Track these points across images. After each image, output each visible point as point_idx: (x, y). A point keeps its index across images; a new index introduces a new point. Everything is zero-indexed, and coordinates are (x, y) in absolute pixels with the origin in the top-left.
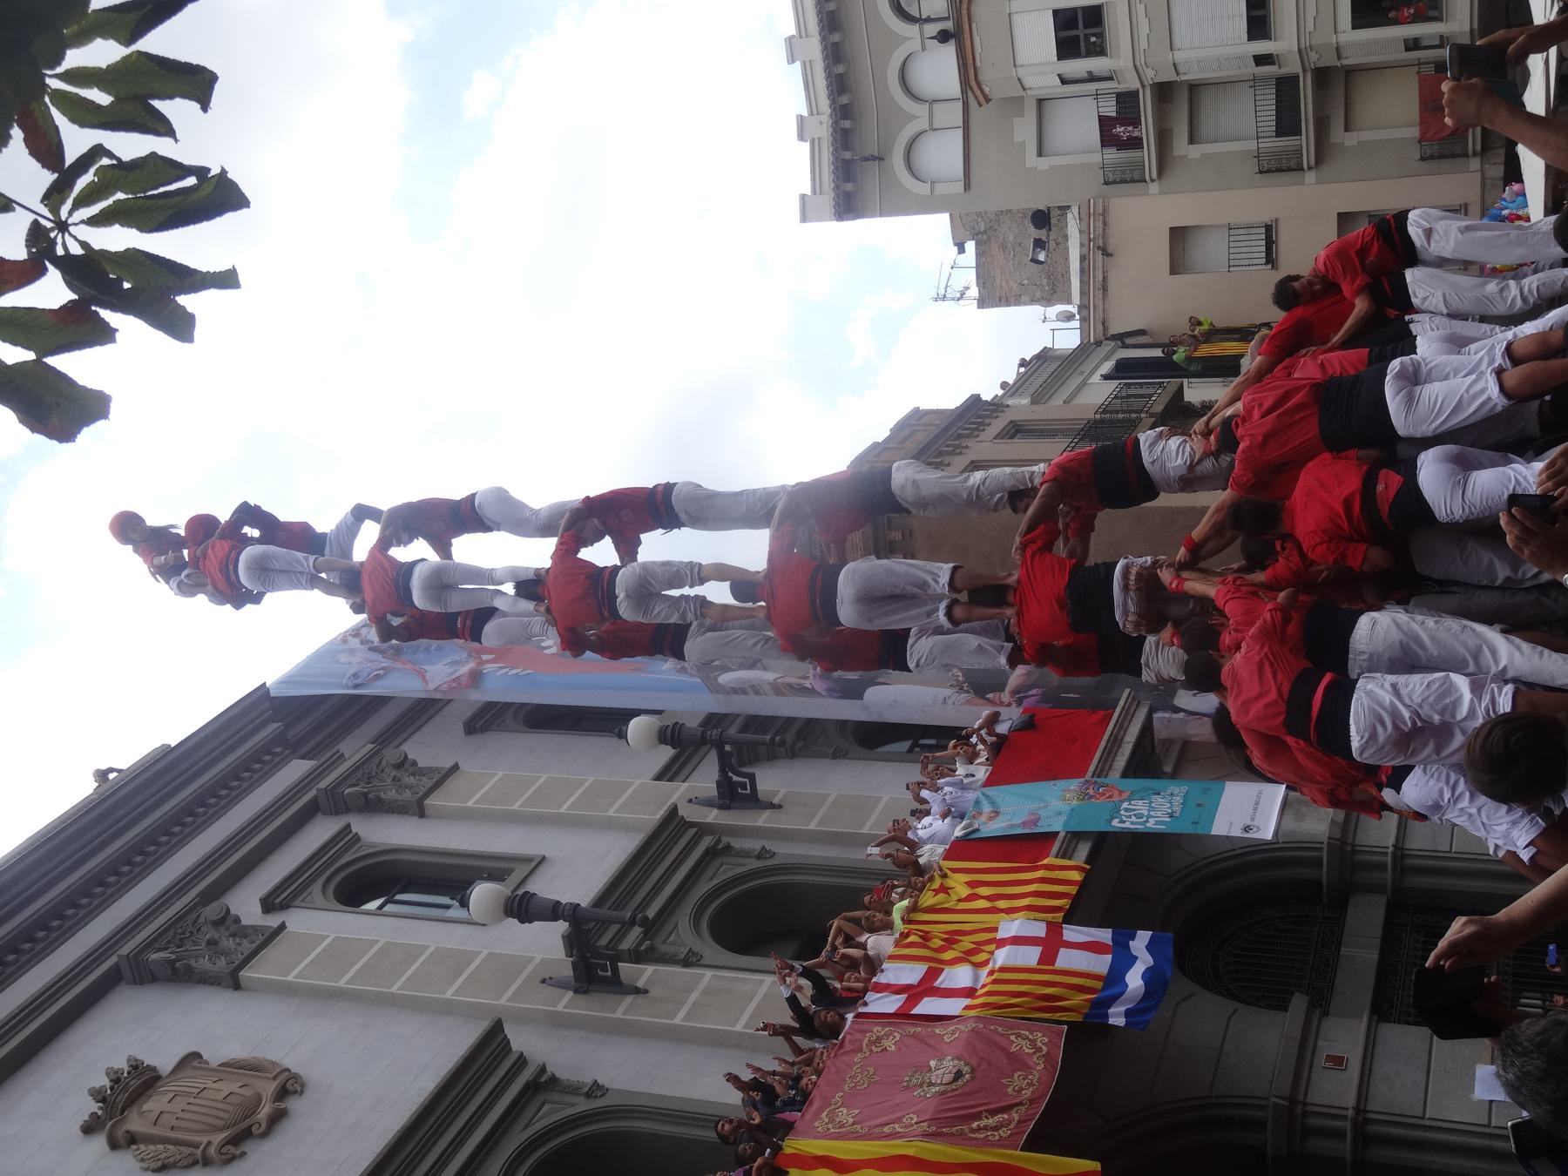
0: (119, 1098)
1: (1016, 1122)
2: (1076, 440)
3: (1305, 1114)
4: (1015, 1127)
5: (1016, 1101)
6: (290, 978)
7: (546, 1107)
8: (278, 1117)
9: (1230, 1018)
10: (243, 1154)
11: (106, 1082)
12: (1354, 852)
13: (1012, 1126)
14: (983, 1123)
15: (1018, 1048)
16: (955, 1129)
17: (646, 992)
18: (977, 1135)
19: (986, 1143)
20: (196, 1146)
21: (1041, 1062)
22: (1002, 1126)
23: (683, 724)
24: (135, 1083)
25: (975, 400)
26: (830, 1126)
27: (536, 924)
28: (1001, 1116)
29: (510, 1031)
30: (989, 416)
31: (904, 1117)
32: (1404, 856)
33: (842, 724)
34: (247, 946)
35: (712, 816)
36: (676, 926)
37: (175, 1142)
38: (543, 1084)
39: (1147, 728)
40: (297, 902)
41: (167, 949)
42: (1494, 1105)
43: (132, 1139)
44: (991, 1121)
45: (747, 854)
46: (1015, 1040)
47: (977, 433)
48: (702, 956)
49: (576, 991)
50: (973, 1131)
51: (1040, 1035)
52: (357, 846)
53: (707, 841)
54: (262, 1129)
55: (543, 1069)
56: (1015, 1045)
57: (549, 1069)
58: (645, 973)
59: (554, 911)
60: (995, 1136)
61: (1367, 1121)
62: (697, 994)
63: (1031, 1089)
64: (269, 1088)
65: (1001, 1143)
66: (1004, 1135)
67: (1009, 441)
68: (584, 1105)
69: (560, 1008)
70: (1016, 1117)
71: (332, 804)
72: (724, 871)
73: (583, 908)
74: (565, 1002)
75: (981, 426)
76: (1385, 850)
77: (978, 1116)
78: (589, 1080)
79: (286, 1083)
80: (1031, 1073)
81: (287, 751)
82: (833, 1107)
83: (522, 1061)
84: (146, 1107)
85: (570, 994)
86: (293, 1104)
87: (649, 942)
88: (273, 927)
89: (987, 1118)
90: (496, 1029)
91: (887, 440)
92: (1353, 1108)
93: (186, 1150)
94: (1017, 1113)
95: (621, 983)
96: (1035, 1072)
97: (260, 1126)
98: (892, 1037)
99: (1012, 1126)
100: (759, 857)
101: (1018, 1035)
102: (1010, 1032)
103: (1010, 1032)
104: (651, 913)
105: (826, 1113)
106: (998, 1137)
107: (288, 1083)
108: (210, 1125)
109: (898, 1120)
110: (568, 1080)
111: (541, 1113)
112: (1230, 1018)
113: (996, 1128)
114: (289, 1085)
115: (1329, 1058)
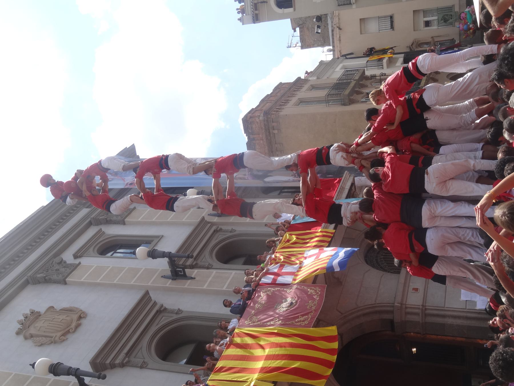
0: (27, 324)
1: (310, 318)
2: (331, 90)
3: (406, 308)
4: (310, 320)
5: (310, 311)
6: (82, 280)
7: (164, 318)
8: (78, 326)
9: (381, 277)
10: (67, 339)
11: (23, 318)
13: (309, 320)
14: (299, 320)
15: (311, 293)
16: (290, 322)
17: (195, 278)
18: (298, 324)
19: (300, 326)
20: (52, 337)
21: (318, 297)
22: (306, 320)
23: (205, 191)
25: (299, 79)
26: (250, 322)
27: (158, 259)
28: (305, 316)
29: (152, 294)
30: (303, 84)
33: (257, 188)
34: (68, 271)
35: (216, 219)
38: (162, 310)
39: (353, 184)
40: (85, 255)
41: (43, 273)
42: (467, 302)
43: (32, 336)
44: (302, 319)
45: (227, 231)
46: (310, 291)
47: (300, 89)
48: (213, 265)
49: (172, 280)
50: (296, 322)
51: (318, 288)
52: (104, 235)
53: (214, 228)
55: (162, 306)
57: (164, 306)
58: (194, 273)
59: (163, 255)
60: (303, 324)
61: (426, 309)
62: (209, 280)
63: (315, 307)
64: (75, 317)
65: (306, 326)
66: (306, 323)
67: (310, 91)
68: (175, 317)
69: (167, 285)
70: (310, 316)
71: (96, 222)
72: (219, 237)
73: (173, 254)
74: (169, 283)
75: (301, 87)
77: (298, 317)
78: (177, 308)
79: (81, 315)
80: (315, 301)
81: (81, 206)
82: (251, 316)
83: (155, 303)
84: (37, 325)
85: (171, 280)
86: (83, 321)
87: (196, 262)
88: (76, 264)
89: (301, 318)
90: (147, 293)
91: (272, 93)
92: (422, 305)
93: (48, 339)
95: (187, 276)
96: (316, 301)
97: (72, 329)
99: (309, 320)
100: (231, 232)
101: (311, 289)
102: (308, 288)
103: (308, 288)
104: (195, 254)
105: (249, 318)
106: (304, 324)
107: (81, 315)
110: (170, 309)
111: (162, 320)
112: (381, 277)
113: (304, 321)
114: (82, 316)
115: (414, 289)
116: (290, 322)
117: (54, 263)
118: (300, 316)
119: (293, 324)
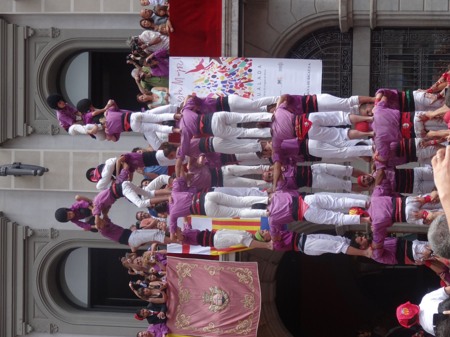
1: (251, 324)
12: (354, 15)
18: (239, 333)
22: (247, 327)
26: (181, 325)
31: (208, 323)
32: (377, 16)
36: (35, 104)
51: (248, 270)
56: (240, 279)
60: (246, 332)
63: (253, 304)
76: (368, 13)
77: (236, 323)
89: (240, 322)
94: (251, 318)
98: (188, 269)
109: (207, 325)
113: (245, 329)
116: (230, 331)
118: (239, 321)
119: (234, 334)
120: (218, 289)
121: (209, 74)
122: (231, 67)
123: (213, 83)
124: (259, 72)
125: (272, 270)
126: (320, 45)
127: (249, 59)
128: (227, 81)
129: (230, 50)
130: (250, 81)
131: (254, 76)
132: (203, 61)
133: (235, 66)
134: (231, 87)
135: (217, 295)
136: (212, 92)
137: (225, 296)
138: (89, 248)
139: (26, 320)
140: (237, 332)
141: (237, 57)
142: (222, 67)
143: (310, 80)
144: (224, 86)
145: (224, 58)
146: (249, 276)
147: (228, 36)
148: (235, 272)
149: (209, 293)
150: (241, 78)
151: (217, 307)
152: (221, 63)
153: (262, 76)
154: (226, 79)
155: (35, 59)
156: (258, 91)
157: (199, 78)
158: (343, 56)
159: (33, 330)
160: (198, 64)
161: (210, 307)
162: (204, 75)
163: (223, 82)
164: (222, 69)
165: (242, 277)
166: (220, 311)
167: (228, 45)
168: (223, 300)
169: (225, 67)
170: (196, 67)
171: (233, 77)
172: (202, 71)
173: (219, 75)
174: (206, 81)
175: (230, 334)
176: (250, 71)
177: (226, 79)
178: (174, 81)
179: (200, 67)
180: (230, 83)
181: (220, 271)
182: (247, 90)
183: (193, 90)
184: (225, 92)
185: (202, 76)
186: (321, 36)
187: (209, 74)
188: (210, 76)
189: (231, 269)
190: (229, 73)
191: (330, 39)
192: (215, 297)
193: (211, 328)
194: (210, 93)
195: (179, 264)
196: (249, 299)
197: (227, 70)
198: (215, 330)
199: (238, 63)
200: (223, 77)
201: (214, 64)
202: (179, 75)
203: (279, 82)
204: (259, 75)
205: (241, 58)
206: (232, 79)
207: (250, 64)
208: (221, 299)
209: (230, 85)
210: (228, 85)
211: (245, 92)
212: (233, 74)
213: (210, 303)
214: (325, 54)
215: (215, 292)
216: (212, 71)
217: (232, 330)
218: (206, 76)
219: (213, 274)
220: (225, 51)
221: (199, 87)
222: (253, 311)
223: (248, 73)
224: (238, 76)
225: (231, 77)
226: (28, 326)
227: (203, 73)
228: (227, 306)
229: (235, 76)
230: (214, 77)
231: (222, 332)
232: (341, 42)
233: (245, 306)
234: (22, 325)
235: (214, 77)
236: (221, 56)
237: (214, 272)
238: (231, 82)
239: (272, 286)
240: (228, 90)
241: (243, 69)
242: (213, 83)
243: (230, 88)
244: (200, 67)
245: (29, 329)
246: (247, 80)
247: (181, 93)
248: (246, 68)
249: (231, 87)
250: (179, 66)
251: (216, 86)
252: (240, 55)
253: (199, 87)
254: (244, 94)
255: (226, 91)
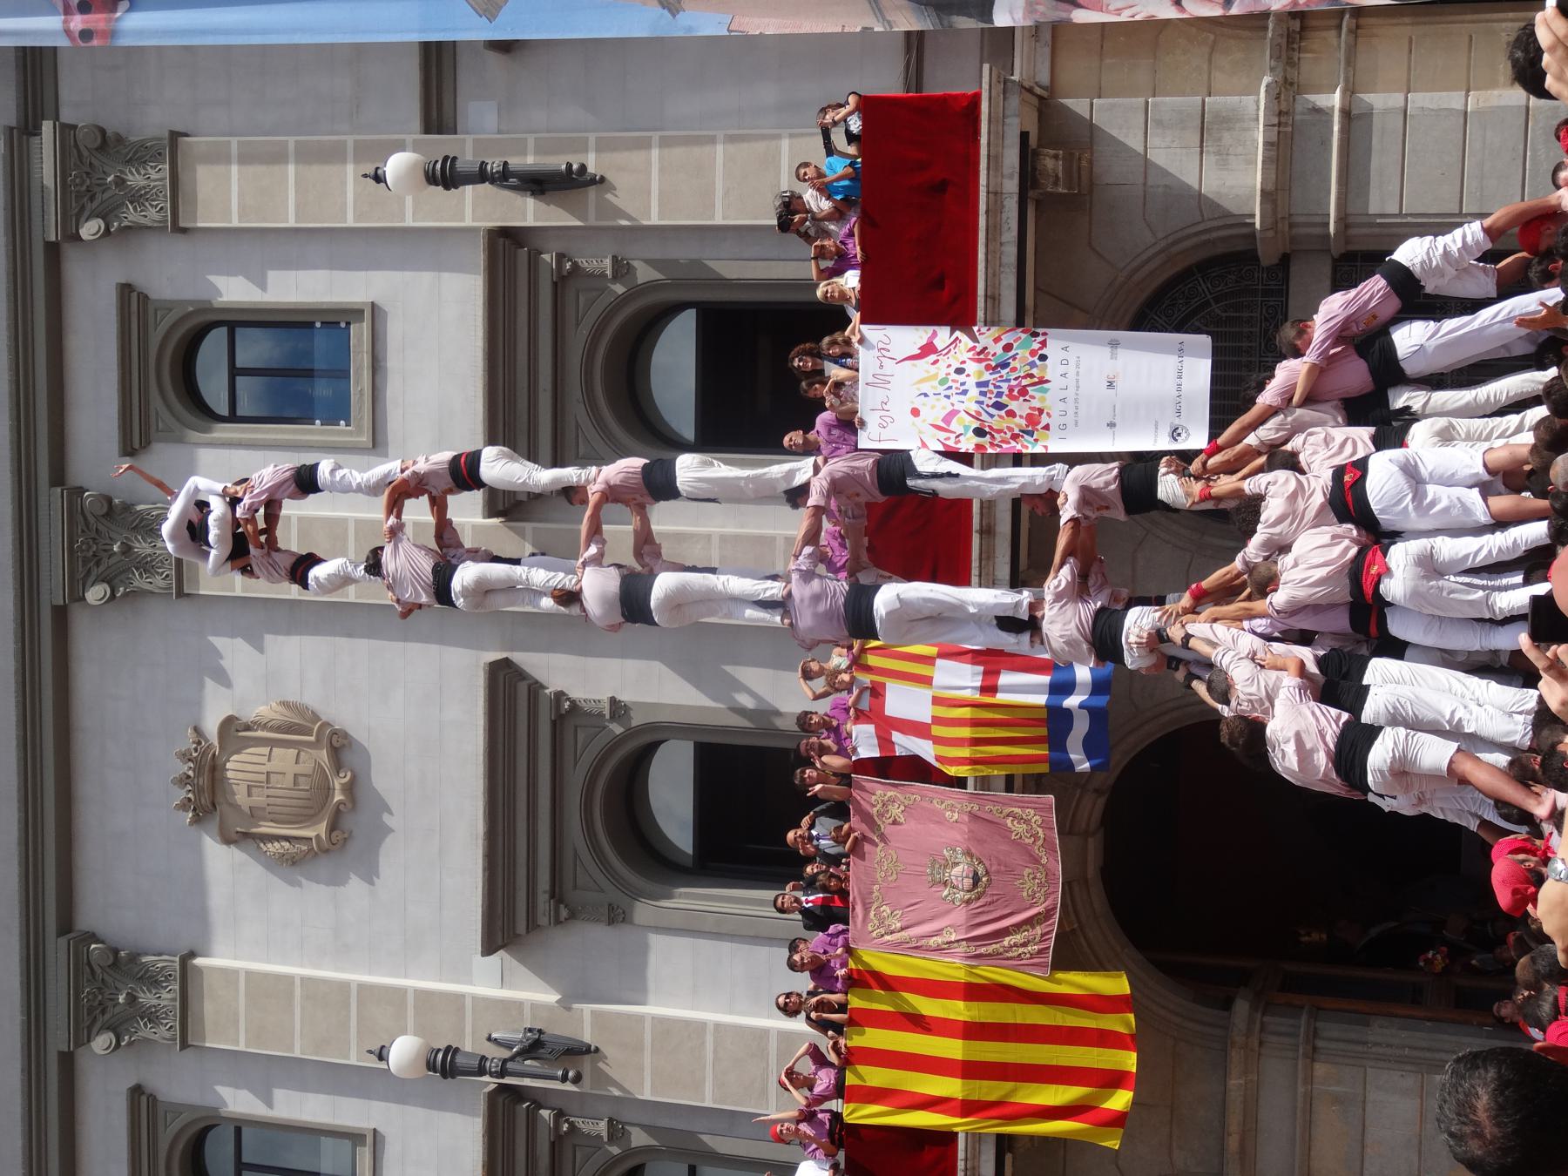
7: (581, 736)
9: (1188, 571)
18: (1010, 954)
22: (1029, 941)
24: (204, 781)
36: (577, 422)
37: (287, 839)
51: (1032, 812)
54: (349, 805)
108: (302, 815)
109: (938, 933)
113: (1024, 945)
116: (990, 949)
117: (91, 520)
120: (963, 854)
121: (949, 366)
122: (998, 348)
123: (958, 385)
124: (1064, 362)
125: (1092, 809)
126: (1211, 294)
127: (1040, 330)
128: (988, 381)
129: (997, 310)
130: (1042, 381)
131: (1052, 370)
132: (935, 334)
133: (1008, 348)
134: (1000, 395)
135: (961, 866)
136: (955, 408)
137: (981, 870)
138: (696, 744)
139: (557, 896)
140: (1007, 952)
141: (1013, 325)
142: (978, 350)
143: (1184, 381)
144: (982, 394)
145: (984, 329)
146: (1034, 826)
147: (992, 278)
148: (1002, 816)
149: (944, 862)
150: (1022, 374)
151: (962, 893)
152: (975, 340)
153: (1071, 370)
154: (987, 376)
155: (578, 325)
156: (1062, 406)
157: (926, 375)
158: (1266, 319)
159: (573, 916)
160: (924, 342)
161: (946, 893)
162: (938, 368)
163: (979, 385)
164: (979, 354)
165: (1020, 828)
166: (968, 902)
167: (993, 298)
168: (976, 879)
169: (986, 348)
170: (920, 349)
171: (1004, 372)
172: (933, 357)
173: (972, 367)
174: (943, 382)
175: (990, 955)
176: (1043, 358)
177: (987, 376)
178: (871, 380)
179: (928, 349)
180: (996, 387)
181: (970, 812)
182: (1036, 403)
183: (912, 402)
184: (984, 407)
185: (933, 369)
186: (1214, 274)
187: (949, 366)
188: (952, 370)
189: (994, 809)
190: (993, 364)
191: (1237, 282)
192: (957, 870)
193: (949, 940)
194: (950, 408)
195: (878, 792)
196: (1034, 879)
197: (990, 357)
198: (956, 945)
199: (1015, 341)
200: (980, 374)
201: (960, 341)
202: (881, 366)
203: (1111, 385)
204: (1062, 369)
205: (1021, 329)
206: (1002, 376)
207: (1044, 344)
208: (971, 875)
209: (995, 391)
210: (992, 392)
211: (1030, 408)
212: (1004, 365)
213: (945, 884)
214: (1224, 315)
215: (957, 861)
216: (957, 359)
217: (994, 946)
218: (942, 369)
219: (954, 819)
220: (985, 314)
221: (926, 395)
222: (1044, 905)
223: (1038, 362)
224: (1014, 369)
225: (999, 372)
226: (562, 906)
227: (936, 362)
228: (984, 892)
229: (1008, 370)
230: (959, 371)
231: (973, 951)
232: (1260, 287)
233: (1025, 894)
234: (547, 905)
235: (959, 371)
236: (975, 324)
237: (956, 815)
238: (998, 384)
239: (1094, 848)
240: (991, 402)
241: (1027, 355)
242: (958, 385)
243: (996, 397)
244: (928, 349)
245: (564, 913)
246: (1036, 380)
247: (885, 407)
248: (1033, 353)
249: (1000, 395)
250: (881, 345)
251: (965, 392)
252: (1020, 322)
253: (926, 395)
254: (1029, 411)
255: (988, 406)
